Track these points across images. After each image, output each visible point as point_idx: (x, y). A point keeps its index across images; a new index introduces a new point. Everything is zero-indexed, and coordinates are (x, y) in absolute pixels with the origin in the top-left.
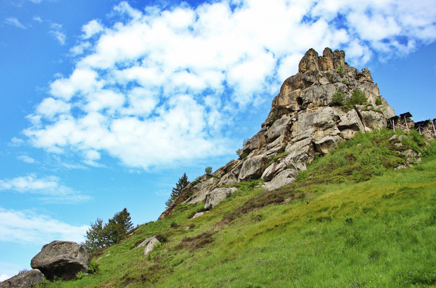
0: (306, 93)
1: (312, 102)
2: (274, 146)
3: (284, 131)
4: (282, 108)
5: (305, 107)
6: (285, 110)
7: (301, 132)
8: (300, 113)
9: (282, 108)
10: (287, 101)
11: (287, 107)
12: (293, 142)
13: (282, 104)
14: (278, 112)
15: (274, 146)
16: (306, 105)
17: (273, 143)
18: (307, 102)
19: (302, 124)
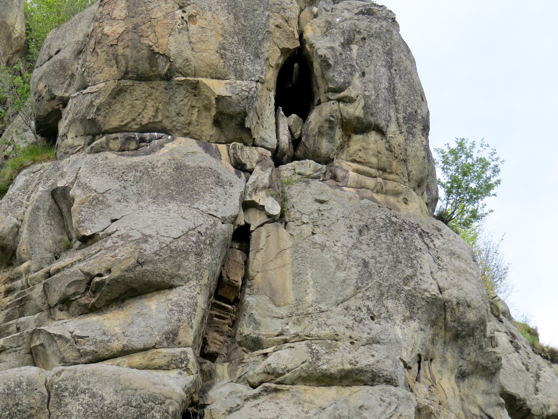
0: (347, 43)
1: (381, 131)
2: (125, 352)
3: (207, 259)
4: (167, 78)
5: (325, 146)
6: (181, 97)
7: (337, 321)
8: (307, 178)
9: (167, 78)
10: (214, 43)
11: (219, 88)
12: (273, 374)
13: (173, 45)
14: (118, 93)
15: (125, 352)
16: (338, 133)
17: (113, 325)
18: (354, 110)
19: (339, 265)
